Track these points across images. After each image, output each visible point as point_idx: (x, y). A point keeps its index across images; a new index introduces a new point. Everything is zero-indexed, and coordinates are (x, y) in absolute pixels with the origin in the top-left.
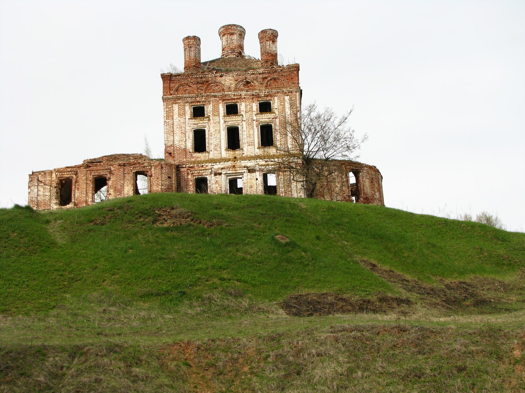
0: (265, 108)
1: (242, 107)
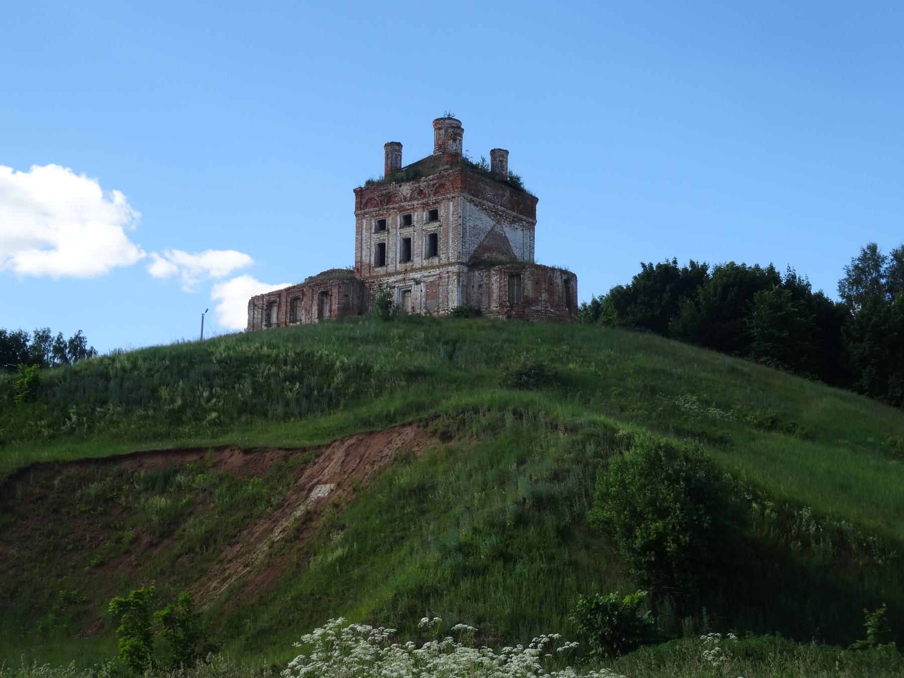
0: (434, 216)
1: (415, 218)
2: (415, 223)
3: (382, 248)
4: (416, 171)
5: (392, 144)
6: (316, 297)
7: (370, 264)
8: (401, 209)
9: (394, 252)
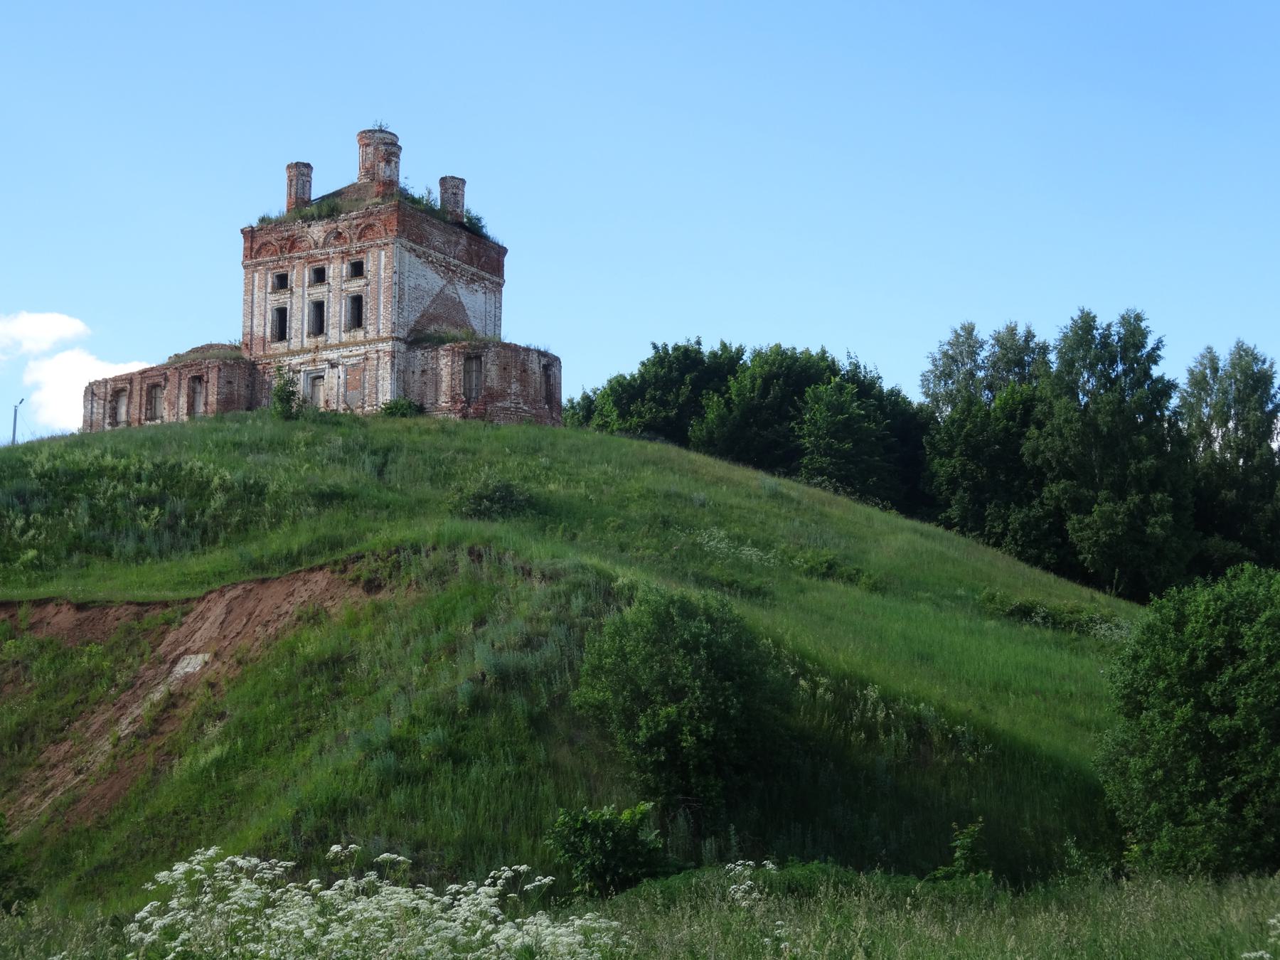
0: (357, 270)
2: (330, 280)
3: (282, 314)
4: (331, 206)
5: (297, 165)
6: (185, 384)
7: (264, 339)
8: (310, 259)
9: (299, 321)
